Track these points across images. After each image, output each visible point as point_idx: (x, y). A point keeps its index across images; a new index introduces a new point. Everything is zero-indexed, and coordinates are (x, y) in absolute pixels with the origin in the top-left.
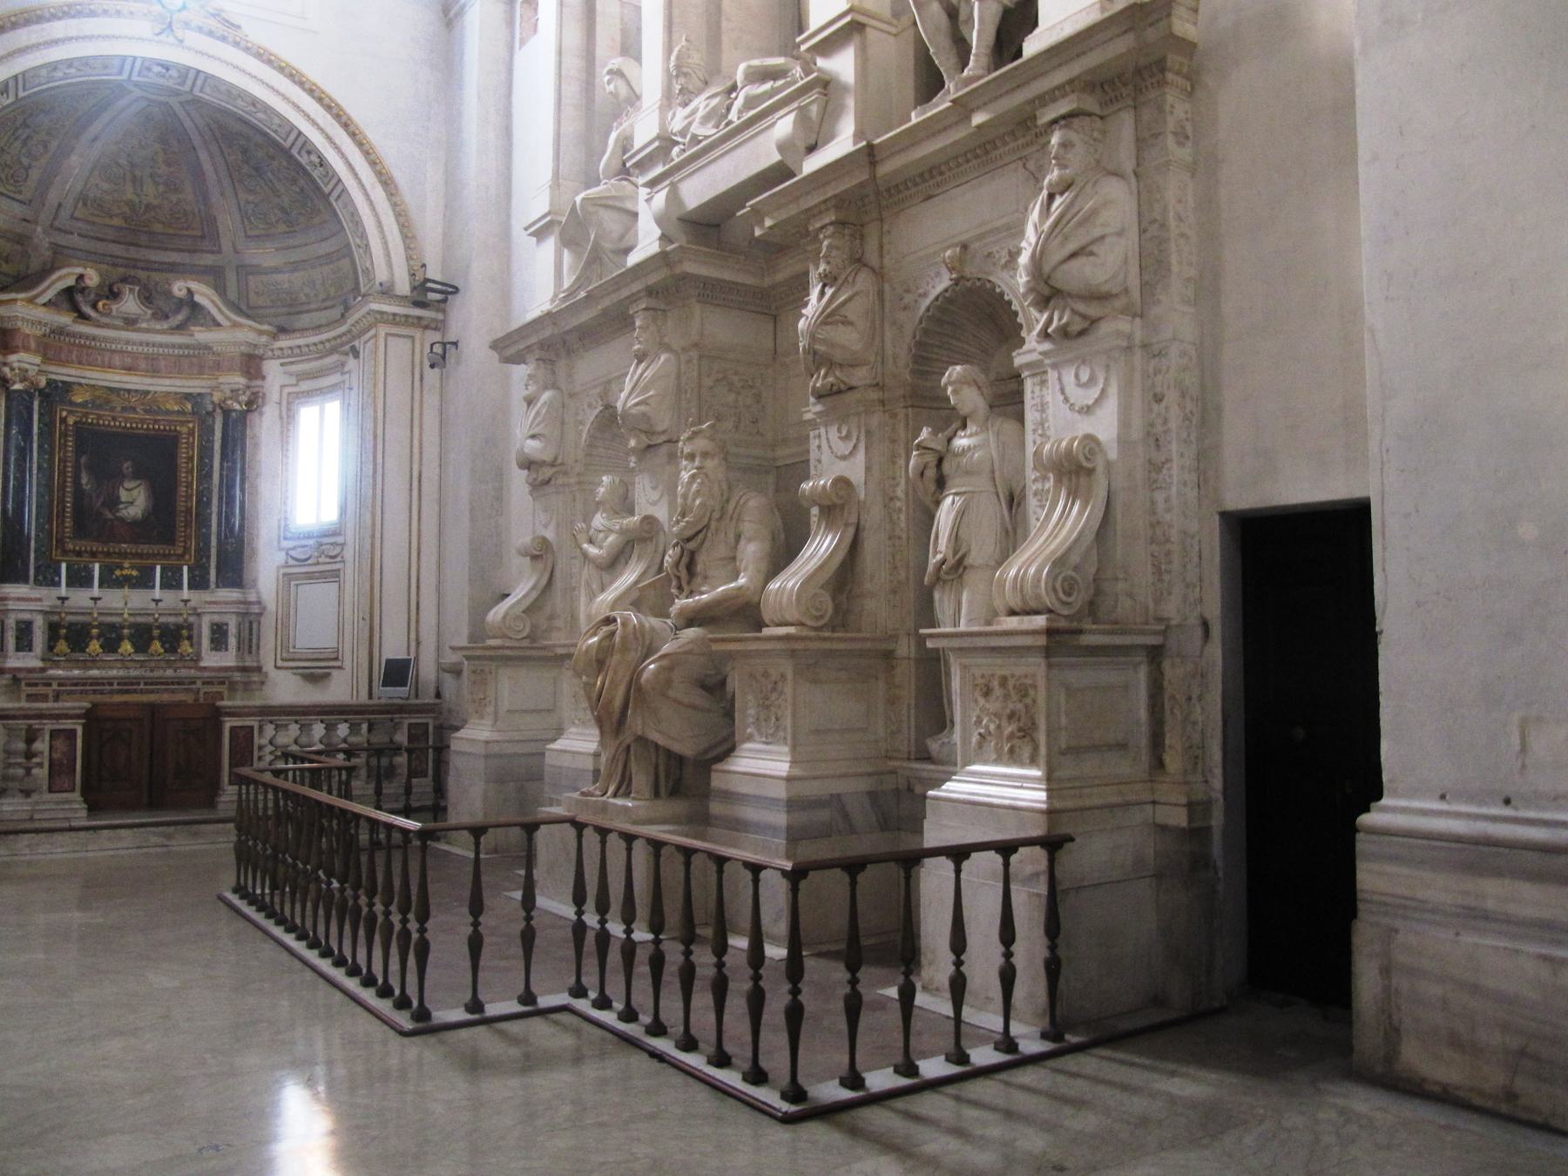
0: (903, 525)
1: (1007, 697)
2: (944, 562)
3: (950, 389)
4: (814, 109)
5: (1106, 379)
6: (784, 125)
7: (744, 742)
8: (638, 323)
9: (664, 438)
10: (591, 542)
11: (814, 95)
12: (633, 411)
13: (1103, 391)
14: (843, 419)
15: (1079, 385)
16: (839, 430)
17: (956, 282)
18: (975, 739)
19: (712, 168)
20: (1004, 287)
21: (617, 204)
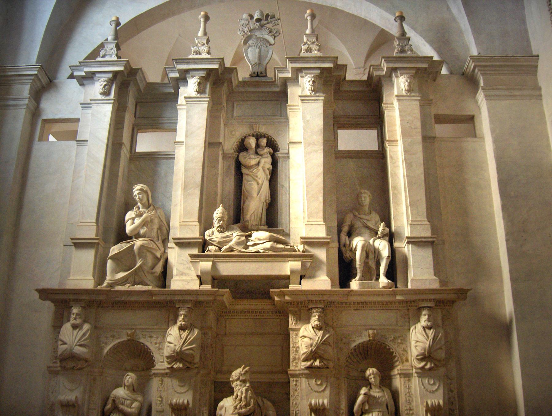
3: (372, 376)
4: (309, 264)
6: (296, 265)
9: (196, 366)
10: (122, 404)
11: (309, 260)
12: (187, 352)
14: (317, 378)
15: (429, 384)
16: (316, 381)
17: (369, 341)
19: (243, 264)
20: (391, 347)
21: (154, 252)
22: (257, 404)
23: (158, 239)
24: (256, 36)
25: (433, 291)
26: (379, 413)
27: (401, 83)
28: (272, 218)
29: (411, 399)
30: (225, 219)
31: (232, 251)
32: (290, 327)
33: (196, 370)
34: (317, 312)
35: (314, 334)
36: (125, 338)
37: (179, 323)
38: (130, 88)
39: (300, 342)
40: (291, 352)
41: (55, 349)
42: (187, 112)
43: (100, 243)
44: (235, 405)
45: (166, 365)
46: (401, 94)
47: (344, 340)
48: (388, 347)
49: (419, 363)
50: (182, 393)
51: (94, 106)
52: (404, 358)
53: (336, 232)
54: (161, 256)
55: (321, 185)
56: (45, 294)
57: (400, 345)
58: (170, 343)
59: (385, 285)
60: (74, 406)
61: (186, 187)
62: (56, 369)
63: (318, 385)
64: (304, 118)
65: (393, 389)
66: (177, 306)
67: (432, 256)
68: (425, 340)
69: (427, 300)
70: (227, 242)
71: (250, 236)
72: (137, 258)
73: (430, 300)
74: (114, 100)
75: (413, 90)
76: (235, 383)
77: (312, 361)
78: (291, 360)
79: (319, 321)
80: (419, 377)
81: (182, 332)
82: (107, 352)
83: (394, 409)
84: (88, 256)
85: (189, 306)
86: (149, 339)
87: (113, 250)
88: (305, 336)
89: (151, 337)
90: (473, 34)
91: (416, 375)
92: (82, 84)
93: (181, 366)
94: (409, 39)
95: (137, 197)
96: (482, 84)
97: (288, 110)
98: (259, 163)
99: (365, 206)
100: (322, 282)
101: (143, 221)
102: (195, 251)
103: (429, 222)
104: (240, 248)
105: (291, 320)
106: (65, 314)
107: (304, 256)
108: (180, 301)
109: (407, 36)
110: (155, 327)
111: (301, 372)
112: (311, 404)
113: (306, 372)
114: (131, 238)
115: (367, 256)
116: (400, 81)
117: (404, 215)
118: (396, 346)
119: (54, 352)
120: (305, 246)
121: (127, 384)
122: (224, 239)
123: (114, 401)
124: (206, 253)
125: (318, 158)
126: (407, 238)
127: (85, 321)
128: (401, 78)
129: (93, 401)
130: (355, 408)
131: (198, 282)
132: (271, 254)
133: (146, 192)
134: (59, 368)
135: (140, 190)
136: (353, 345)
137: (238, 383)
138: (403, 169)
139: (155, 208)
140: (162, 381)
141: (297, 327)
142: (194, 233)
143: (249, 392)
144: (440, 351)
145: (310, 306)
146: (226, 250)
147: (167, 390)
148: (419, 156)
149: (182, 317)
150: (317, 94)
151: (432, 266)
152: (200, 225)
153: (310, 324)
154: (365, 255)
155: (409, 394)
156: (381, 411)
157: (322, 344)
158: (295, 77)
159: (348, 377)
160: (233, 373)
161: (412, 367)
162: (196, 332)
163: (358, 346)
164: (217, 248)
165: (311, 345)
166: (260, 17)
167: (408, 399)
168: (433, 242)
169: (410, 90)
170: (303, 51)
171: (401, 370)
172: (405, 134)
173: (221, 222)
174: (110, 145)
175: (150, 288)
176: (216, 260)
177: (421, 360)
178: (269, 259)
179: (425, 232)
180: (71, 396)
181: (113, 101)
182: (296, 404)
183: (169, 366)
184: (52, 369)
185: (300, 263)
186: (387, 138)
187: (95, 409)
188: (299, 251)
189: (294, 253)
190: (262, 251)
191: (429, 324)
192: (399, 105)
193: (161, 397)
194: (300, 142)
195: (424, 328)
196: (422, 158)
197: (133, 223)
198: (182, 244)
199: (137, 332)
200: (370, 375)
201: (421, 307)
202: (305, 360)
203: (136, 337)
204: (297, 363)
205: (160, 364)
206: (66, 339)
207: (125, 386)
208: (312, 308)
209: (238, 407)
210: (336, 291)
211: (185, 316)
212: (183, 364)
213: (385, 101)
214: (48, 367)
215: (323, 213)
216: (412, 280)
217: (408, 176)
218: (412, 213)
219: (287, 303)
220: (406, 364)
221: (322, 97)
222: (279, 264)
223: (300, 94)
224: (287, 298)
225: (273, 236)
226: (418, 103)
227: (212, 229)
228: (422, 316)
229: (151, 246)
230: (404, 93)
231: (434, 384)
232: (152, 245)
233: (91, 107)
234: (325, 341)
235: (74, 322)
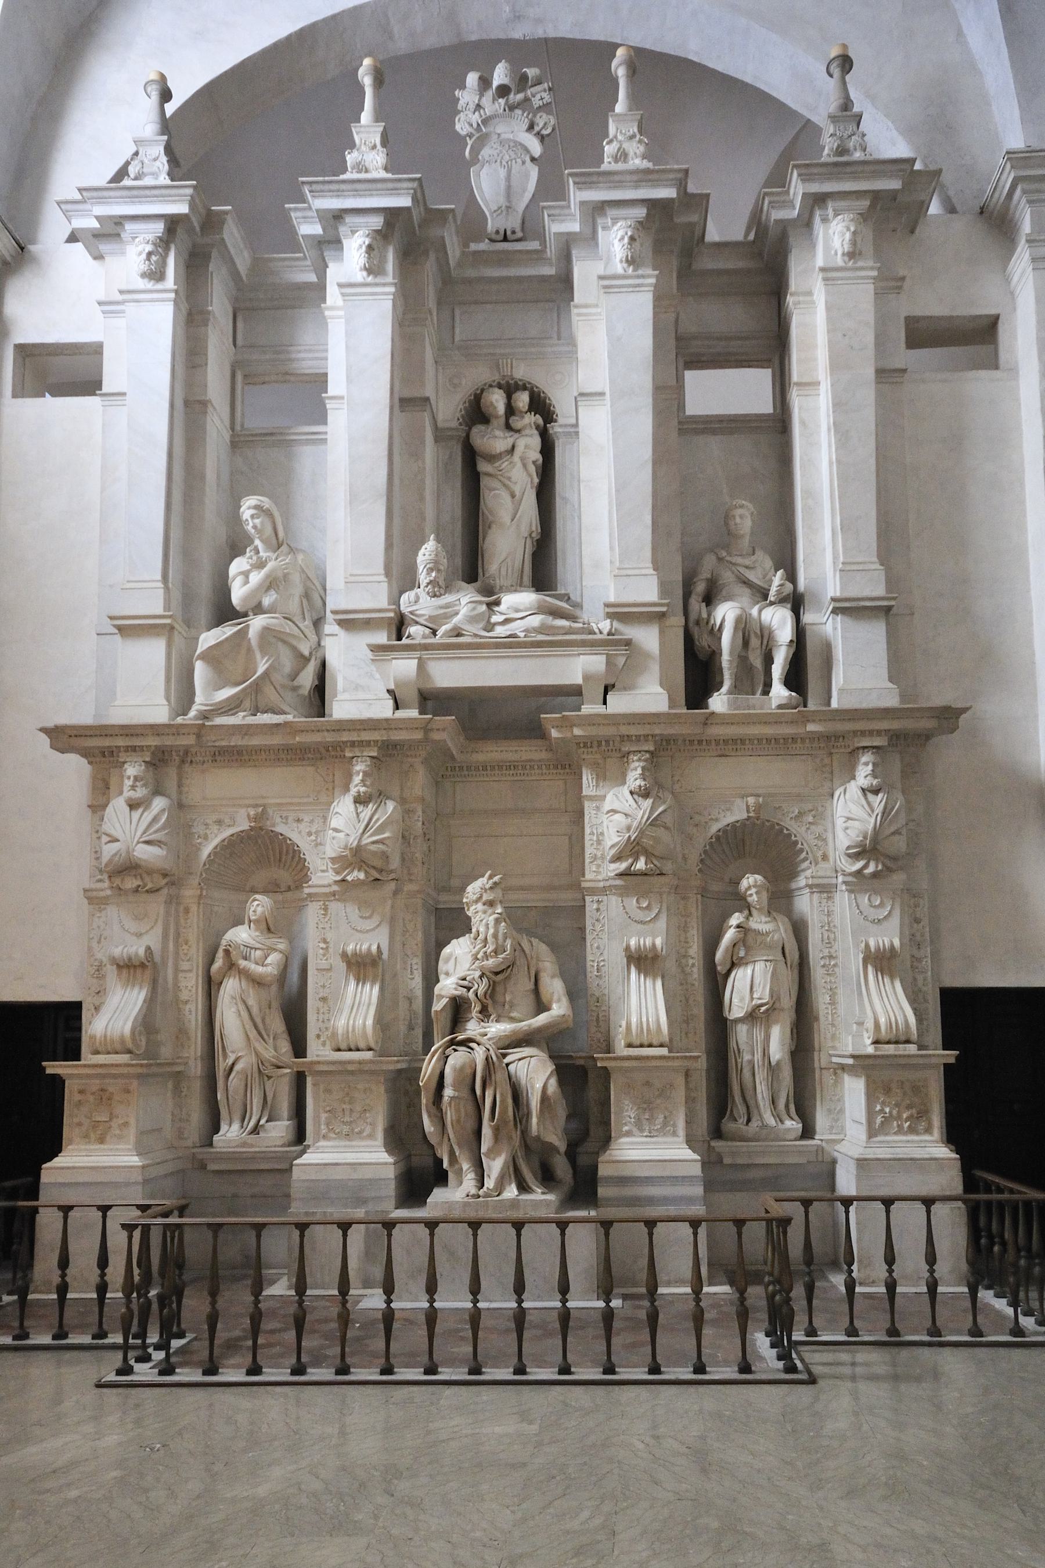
0: (696, 976)
1: (905, 1094)
2: (762, 1005)
3: (753, 891)
4: (621, 661)
5: (893, 905)
6: (594, 662)
7: (620, 1137)
8: (360, 767)
11: (622, 651)
12: (373, 848)
13: (890, 912)
14: (641, 895)
16: (638, 901)
17: (749, 818)
18: (879, 1119)
19: (483, 662)
21: (294, 643)
22: (518, 948)
23: (304, 618)
25: (886, 713)
26: (768, 964)
27: (835, 235)
28: (542, 569)
29: (832, 936)
30: (442, 568)
31: (459, 635)
32: (584, 793)
33: (392, 885)
34: (639, 760)
35: (635, 806)
36: (244, 825)
37: (353, 791)
38: (211, 267)
39: (605, 824)
40: (587, 844)
41: (97, 854)
42: (347, 322)
43: (176, 626)
44: (474, 951)
45: (331, 877)
46: (831, 265)
47: (697, 818)
48: (785, 831)
49: (852, 864)
50: (368, 931)
52: (820, 854)
53: (679, 592)
54: (311, 654)
55: (648, 488)
56: (63, 738)
57: (813, 827)
58: (336, 830)
59: (784, 702)
60: (143, 966)
61: (353, 498)
62: (102, 894)
63: (639, 908)
64: (610, 330)
65: (795, 917)
66: (348, 754)
67: (885, 640)
68: (866, 816)
69: (871, 733)
70: (448, 617)
71: (497, 603)
72: (258, 656)
73: (879, 733)
75: (860, 254)
76: (472, 908)
77: (630, 861)
78: (587, 861)
79: (644, 780)
80: (850, 891)
81: (360, 808)
82: (209, 856)
83: (797, 956)
84: (153, 653)
85: (375, 754)
86: (295, 825)
87: (205, 640)
88: (615, 811)
89: (298, 820)
90: (1018, 95)
91: (844, 887)
92: (99, 257)
93: (362, 876)
94: (858, 118)
95: (251, 524)
96: (1026, 227)
97: (575, 318)
98: (513, 447)
99: (743, 536)
100: (651, 695)
101: (267, 576)
102: (382, 638)
103: (882, 565)
104: (477, 629)
105: (587, 778)
106: (113, 781)
107: (612, 643)
108: (353, 744)
109: (856, 109)
110: (305, 800)
111: (608, 884)
112: (628, 948)
113: (618, 882)
115: (746, 643)
116: (831, 232)
117: (829, 549)
118: (804, 829)
119: (97, 859)
120: (616, 624)
121: (253, 918)
122: (442, 611)
123: (227, 952)
124: (404, 641)
125: (642, 425)
126: (833, 600)
127: (157, 792)
128: (835, 222)
129: (186, 954)
130: (719, 955)
131: (391, 702)
132: (542, 642)
133: (268, 513)
134: (109, 892)
135: (256, 507)
136: (714, 828)
137: (480, 906)
138: (830, 446)
139: (292, 550)
140: (326, 909)
141: (598, 793)
142: (375, 597)
143: (503, 924)
144: (897, 838)
145: (625, 749)
146: (447, 634)
148: (869, 414)
149: (360, 777)
150: (640, 272)
151: (885, 663)
152: (389, 583)
153: (626, 787)
154: (740, 641)
155: (829, 927)
156: (771, 961)
157: (650, 824)
158: (588, 231)
159: (704, 892)
160: (469, 889)
161: (836, 871)
162: (390, 806)
163: (724, 831)
164: (427, 631)
165: (629, 829)
167: (826, 937)
168: (888, 609)
169: (852, 255)
171: (812, 877)
172: (836, 365)
173: (434, 574)
174: (179, 403)
175: (289, 718)
176: (426, 655)
177: (856, 856)
178: (539, 651)
179: (872, 586)
180: (137, 949)
182: (598, 948)
183: (339, 878)
184: (95, 894)
185: (603, 659)
186: (795, 378)
187: (190, 971)
188: (601, 633)
189: (590, 637)
190: (522, 635)
191: (875, 782)
192: (827, 293)
193: (325, 941)
194: (602, 394)
195: (863, 790)
196: (872, 418)
197: (247, 582)
198: (350, 623)
199: (270, 811)
200: (749, 888)
201: (858, 748)
202: (617, 858)
203: (268, 823)
204: (599, 866)
205: (320, 874)
206: (117, 833)
207: (250, 921)
209: (479, 956)
210: (678, 716)
211: (366, 774)
212: (366, 872)
213: (793, 287)
214: (85, 890)
215: (653, 549)
216: (841, 691)
217: (838, 461)
218: (843, 546)
219: (578, 744)
220: (823, 865)
221: (650, 277)
222: (560, 660)
223: (602, 273)
224: (577, 731)
225: (546, 601)
226: (872, 286)
227: (416, 590)
228: (860, 767)
229: (288, 631)
230: (839, 261)
231: (882, 905)
232: (289, 628)
233: (123, 312)
234: (656, 819)
235: (132, 794)
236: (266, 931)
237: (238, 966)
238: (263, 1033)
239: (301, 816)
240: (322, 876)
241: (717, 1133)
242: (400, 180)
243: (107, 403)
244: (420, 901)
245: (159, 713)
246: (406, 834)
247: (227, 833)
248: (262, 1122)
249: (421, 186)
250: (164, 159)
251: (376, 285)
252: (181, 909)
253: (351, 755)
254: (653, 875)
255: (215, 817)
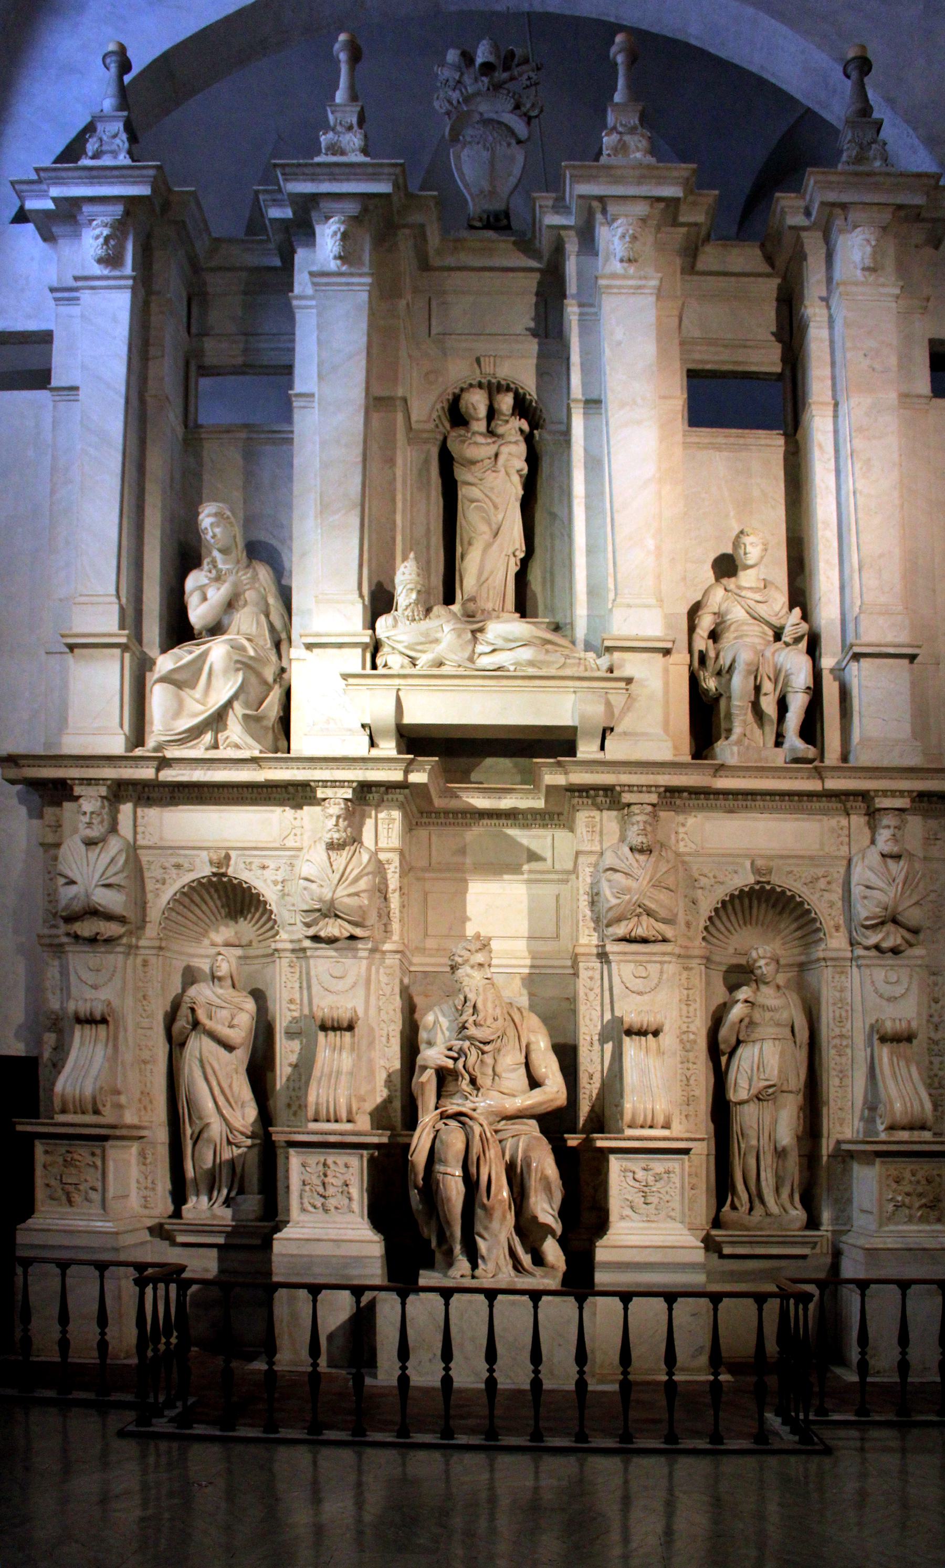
24: (481, 114)
41: (52, 897)
51: (86, 296)
74: (134, 278)
86: (260, 872)
89: (264, 867)
95: (211, 534)
114: (200, 636)
119: (50, 902)
124: (381, 671)
135: (216, 515)
147: (309, 987)
166: (492, 59)
170: (605, 152)
181: (130, 282)
197: (205, 599)
208: (629, 805)
236: (231, 990)
237: (204, 1026)
238: (231, 1100)
239: (267, 862)
240: (292, 931)
241: (717, 1223)
242: (381, 165)
243: (58, 398)
244: (397, 962)
245: (116, 745)
246: (382, 887)
247: (188, 878)
248: (233, 1194)
249: (404, 172)
250: (124, 136)
251: (352, 275)
252: (139, 960)
253: (323, 796)
254: (655, 941)
255: (174, 860)
